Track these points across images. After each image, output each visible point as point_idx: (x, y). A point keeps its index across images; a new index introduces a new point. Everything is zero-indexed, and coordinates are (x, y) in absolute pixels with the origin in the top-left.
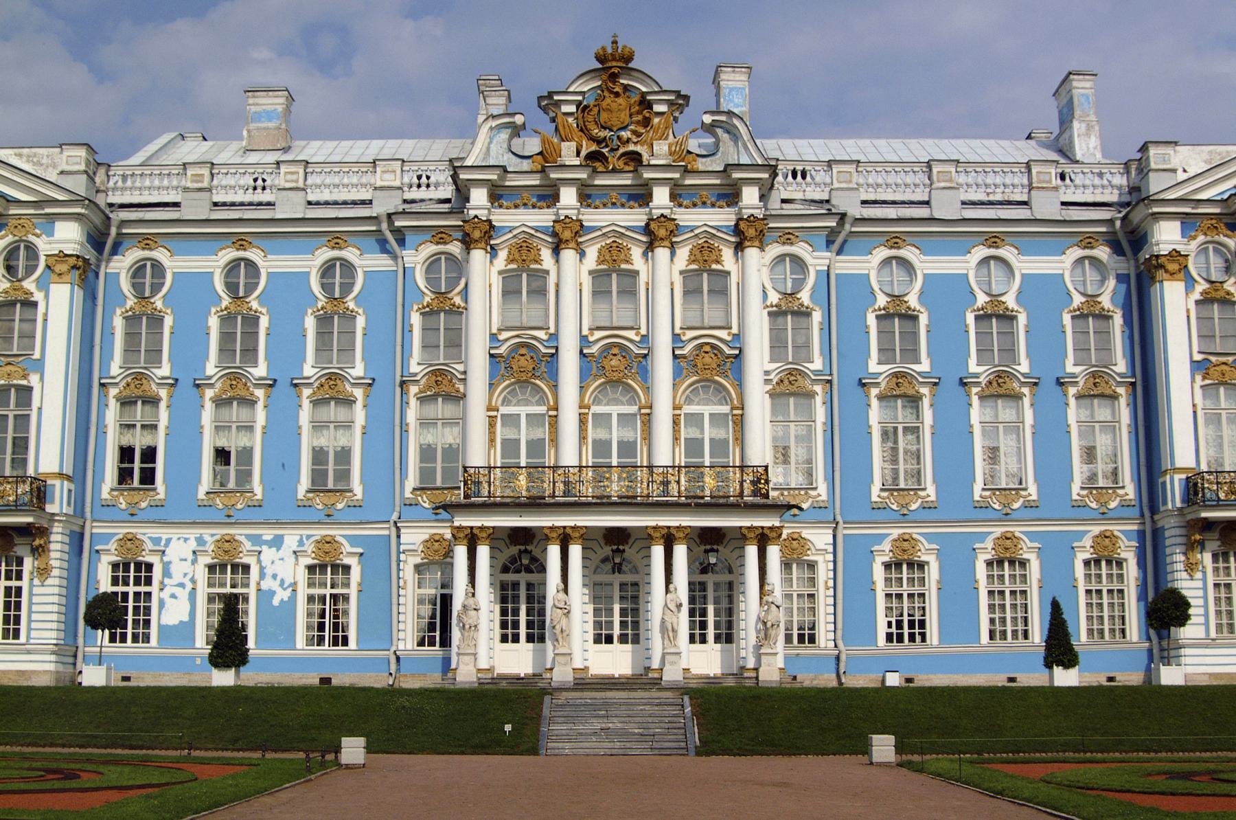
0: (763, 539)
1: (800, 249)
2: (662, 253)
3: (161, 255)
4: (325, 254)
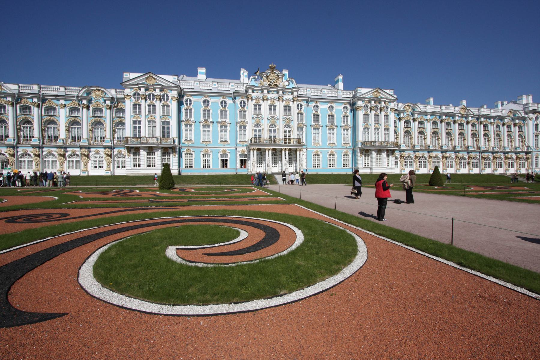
3: (191, 98)
4: (221, 99)
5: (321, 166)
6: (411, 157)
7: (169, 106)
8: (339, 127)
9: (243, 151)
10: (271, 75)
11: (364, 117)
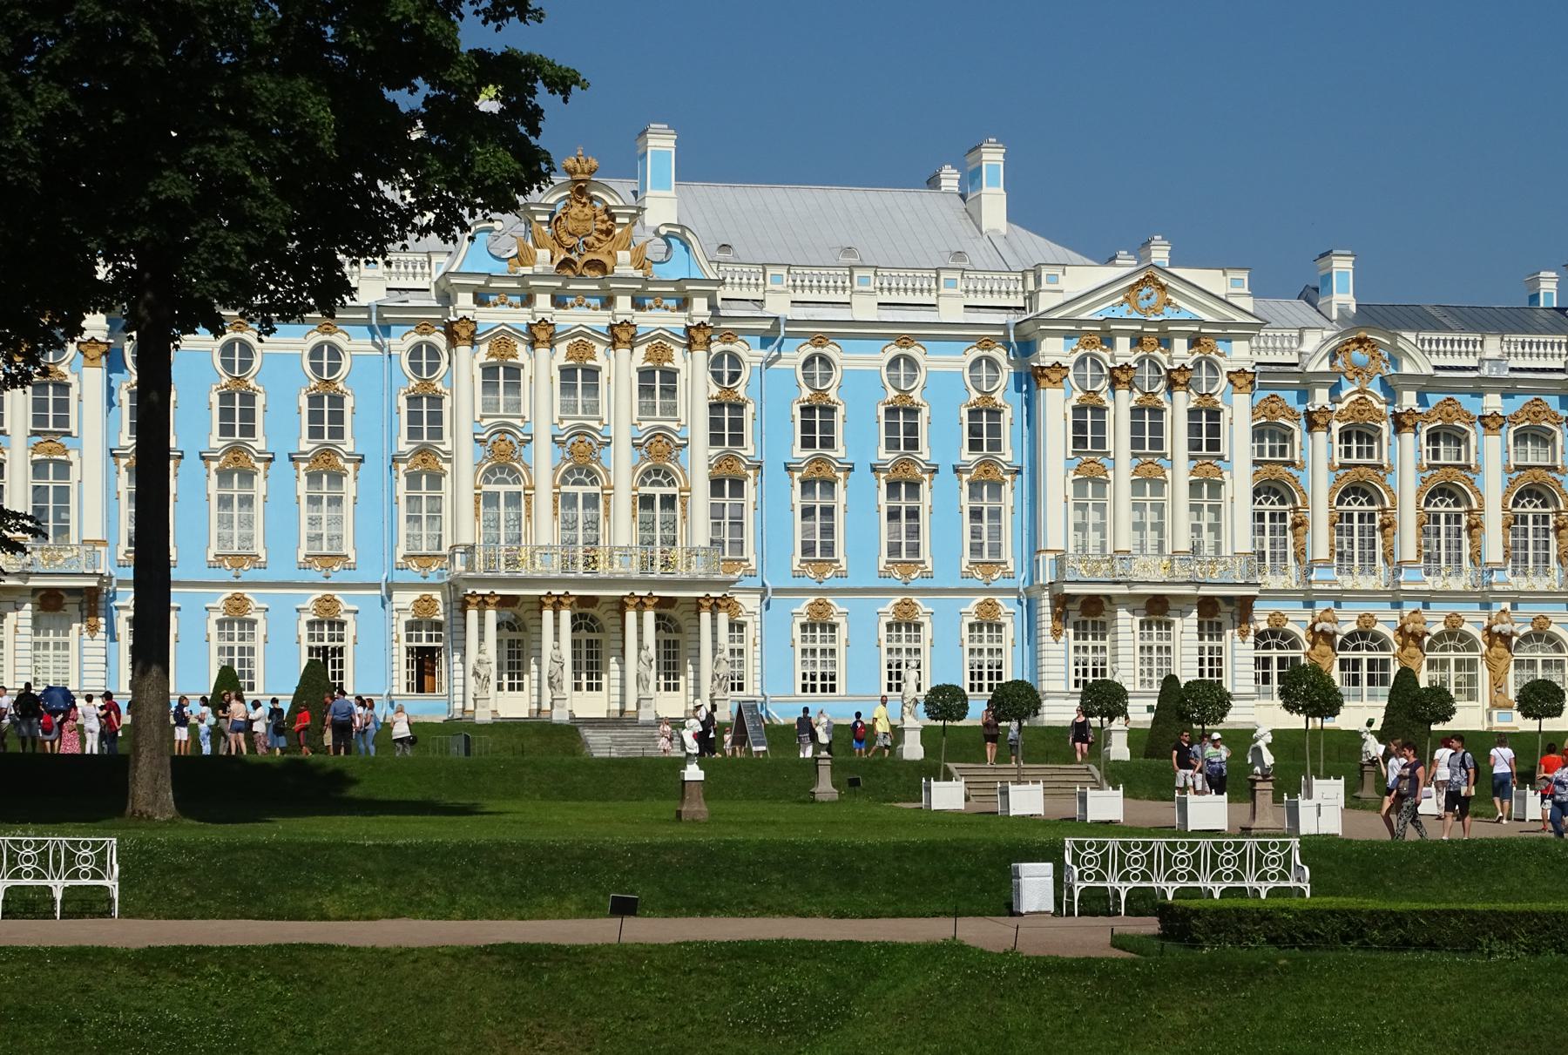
0: (715, 606)
1: (737, 348)
2: (623, 352)
5: (840, 683)
6: (1465, 637)
7: (68, 386)
8: (946, 471)
9: (425, 604)
10: (576, 210)
11: (1079, 427)
